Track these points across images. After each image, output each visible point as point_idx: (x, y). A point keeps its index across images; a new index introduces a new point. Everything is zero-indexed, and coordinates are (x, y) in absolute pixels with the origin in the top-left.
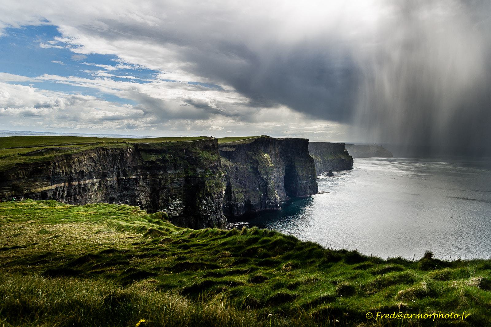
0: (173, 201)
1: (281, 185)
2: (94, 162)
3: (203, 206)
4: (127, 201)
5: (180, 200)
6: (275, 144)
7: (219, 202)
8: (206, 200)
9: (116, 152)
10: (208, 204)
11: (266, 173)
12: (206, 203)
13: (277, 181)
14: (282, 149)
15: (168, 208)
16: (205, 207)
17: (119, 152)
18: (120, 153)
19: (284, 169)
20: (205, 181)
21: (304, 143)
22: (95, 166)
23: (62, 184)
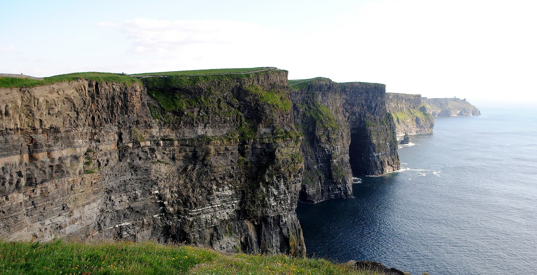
0: (219, 191)
2: (75, 111)
3: (272, 199)
4: (135, 194)
5: (231, 189)
8: (277, 188)
9: (114, 90)
10: (280, 193)
11: (329, 140)
12: (276, 193)
14: (346, 100)
15: (211, 205)
16: (275, 200)
17: (118, 90)
18: (120, 93)
19: (350, 134)
20: (275, 150)
22: (77, 118)
23: (16, 159)
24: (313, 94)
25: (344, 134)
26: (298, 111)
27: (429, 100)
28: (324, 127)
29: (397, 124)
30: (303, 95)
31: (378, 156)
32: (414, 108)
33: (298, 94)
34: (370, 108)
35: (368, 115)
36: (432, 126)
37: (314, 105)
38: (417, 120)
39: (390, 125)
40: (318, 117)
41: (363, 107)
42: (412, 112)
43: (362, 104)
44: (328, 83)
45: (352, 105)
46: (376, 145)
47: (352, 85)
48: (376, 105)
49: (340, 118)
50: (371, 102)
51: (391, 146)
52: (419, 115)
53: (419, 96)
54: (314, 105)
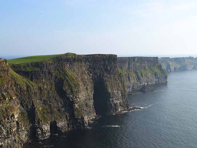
1: (91, 103)
6: (81, 62)
7: (10, 126)
11: (72, 92)
13: (86, 100)
14: (90, 66)
21: (112, 58)
24: (62, 64)
25: (88, 87)
26: (52, 75)
27: (171, 59)
28: (69, 84)
29: (141, 78)
30: (55, 65)
31: (112, 101)
32: (154, 66)
33: (52, 64)
34: (107, 70)
35: (105, 74)
36: (166, 77)
37: (63, 71)
38: (156, 74)
39: (121, 80)
40: (65, 79)
41: (102, 70)
42: (152, 69)
43: (101, 68)
44: (74, 57)
45: (94, 69)
46: (111, 93)
47: (93, 55)
48: (111, 69)
49: (86, 77)
50: (107, 66)
51: (122, 93)
52: (157, 70)
53: (157, 58)
54: (63, 71)
